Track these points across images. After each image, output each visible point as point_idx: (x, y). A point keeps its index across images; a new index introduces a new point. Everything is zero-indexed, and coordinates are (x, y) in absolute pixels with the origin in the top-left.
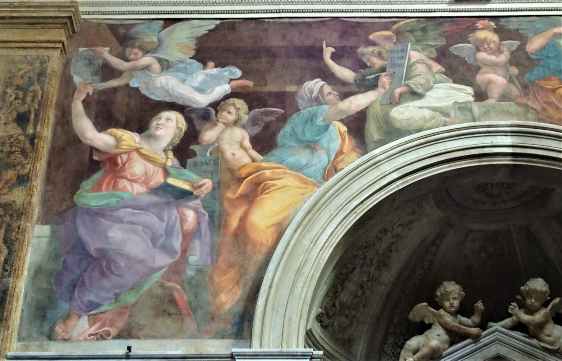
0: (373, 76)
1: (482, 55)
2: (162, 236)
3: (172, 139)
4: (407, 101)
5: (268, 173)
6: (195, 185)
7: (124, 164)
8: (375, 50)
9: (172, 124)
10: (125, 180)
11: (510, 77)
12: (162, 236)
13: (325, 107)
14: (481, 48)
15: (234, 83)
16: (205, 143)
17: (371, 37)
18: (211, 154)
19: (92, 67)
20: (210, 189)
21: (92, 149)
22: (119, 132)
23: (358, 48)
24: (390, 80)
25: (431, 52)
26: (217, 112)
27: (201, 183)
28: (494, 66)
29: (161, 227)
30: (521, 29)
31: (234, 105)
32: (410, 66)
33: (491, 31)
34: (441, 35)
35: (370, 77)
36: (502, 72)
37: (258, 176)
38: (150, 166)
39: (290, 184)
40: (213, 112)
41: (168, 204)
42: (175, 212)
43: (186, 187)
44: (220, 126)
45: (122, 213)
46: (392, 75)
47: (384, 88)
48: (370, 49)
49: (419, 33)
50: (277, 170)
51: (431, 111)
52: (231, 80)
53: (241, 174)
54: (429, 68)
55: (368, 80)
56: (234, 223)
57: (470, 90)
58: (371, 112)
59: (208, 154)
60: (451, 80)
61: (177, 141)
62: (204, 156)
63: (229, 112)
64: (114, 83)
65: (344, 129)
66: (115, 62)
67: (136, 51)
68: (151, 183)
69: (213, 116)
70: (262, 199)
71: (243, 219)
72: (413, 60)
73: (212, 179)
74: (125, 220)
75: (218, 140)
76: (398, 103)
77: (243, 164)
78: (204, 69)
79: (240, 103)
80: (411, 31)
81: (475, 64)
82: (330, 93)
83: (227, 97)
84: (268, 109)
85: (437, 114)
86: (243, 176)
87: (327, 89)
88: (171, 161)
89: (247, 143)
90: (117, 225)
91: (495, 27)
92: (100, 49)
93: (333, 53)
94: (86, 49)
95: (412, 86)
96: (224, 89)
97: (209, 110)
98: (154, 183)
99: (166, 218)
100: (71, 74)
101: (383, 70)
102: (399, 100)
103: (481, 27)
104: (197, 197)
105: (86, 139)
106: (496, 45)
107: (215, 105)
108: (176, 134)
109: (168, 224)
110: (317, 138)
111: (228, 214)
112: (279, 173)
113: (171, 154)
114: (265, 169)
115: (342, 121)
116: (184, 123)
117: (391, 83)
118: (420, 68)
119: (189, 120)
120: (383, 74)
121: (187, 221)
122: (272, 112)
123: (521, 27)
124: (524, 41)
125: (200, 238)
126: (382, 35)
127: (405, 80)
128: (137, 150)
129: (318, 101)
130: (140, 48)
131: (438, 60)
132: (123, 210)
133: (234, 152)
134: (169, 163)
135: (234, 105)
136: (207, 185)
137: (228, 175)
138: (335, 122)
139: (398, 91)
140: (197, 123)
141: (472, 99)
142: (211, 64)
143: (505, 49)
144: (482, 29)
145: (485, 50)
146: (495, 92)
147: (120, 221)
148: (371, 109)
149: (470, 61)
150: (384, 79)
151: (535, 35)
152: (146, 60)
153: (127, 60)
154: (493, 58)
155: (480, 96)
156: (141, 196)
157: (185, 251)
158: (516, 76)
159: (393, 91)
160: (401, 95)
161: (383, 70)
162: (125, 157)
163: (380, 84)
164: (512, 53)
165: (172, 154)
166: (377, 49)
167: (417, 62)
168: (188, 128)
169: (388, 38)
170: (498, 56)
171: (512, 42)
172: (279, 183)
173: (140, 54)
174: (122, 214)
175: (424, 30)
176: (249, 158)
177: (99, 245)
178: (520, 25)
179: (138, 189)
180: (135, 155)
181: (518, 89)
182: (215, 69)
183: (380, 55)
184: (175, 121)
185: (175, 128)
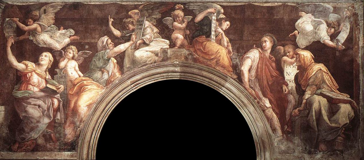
0: (129, 35)
1: (176, 24)
2: (45, 110)
3: (48, 66)
4: (141, 47)
5: (85, 82)
6: (57, 88)
7: (30, 78)
8: (131, 20)
9: (47, 59)
10: (31, 85)
11: (186, 36)
12: (45, 110)
13: (108, 50)
14: (176, 20)
15: (72, 37)
16: (61, 68)
17: (129, 13)
18: (63, 73)
19: (12, 28)
20: (63, 90)
21: (17, 71)
22: (27, 62)
23: (124, 19)
24: (135, 37)
25: (154, 22)
26: (65, 52)
27: (59, 87)
28: (180, 29)
29: (45, 107)
30: (194, 10)
31: (72, 49)
32: (145, 29)
33: (181, 10)
34: (159, 12)
35: (127, 35)
36: (182, 32)
37: (81, 84)
38: (40, 79)
39: (94, 88)
40: (63, 52)
41: (47, 96)
42: (50, 100)
43: (54, 88)
44: (66, 60)
45: (30, 100)
46: (136, 35)
47: (133, 41)
48: (129, 20)
49: (150, 11)
50: (89, 81)
51: (151, 53)
52: (71, 36)
53: (75, 83)
54: (153, 30)
55: (127, 36)
56: (72, 105)
57: (168, 42)
58: (127, 53)
59: (62, 73)
60: (161, 37)
61: (50, 67)
62: (61, 74)
63: (70, 53)
64: (22, 38)
65: (115, 61)
66: (22, 25)
67: (30, 20)
68: (40, 87)
69: (63, 55)
70: (83, 94)
71: (76, 103)
72: (146, 26)
73: (64, 85)
74: (32, 103)
75: (66, 66)
76: (138, 48)
77: (76, 78)
78: (59, 30)
79: (74, 48)
80: (147, 10)
81: (172, 29)
82: (110, 43)
83: (68, 45)
84: (85, 51)
85: (153, 54)
86: (76, 84)
87: (110, 41)
88: (48, 77)
89: (77, 68)
90: (29, 106)
91: (183, 8)
92: (15, 19)
93: (113, 21)
94: (9, 19)
95: (145, 40)
96: (67, 40)
97: (62, 52)
98: (41, 87)
99: (47, 103)
100: (4, 33)
101: (133, 30)
102: (139, 47)
103: (177, 8)
104: (58, 93)
105: (14, 66)
106: (182, 18)
107: (64, 49)
108: (49, 63)
109: (48, 105)
110: (104, 66)
111: (70, 101)
112: (88, 82)
113: (48, 73)
114: (85, 80)
115: (115, 57)
116: (52, 58)
117: (136, 38)
118: (149, 30)
119: (54, 56)
120: (133, 33)
121: (55, 104)
122: (87, 53)
123: (194, 8)
124: (195, 16)
125: (60, 111)
126: (134, 12)
127: (142, 37)
128: (34, 71)
129: (105, 48)
130: (31, 18)
131: (156, 26)
132: (31, 99)
133: (71, 72)
134: (47, 77)
135: (72, 49)
136: (62, 87)
137: (70, 83)
138: (112, 58)
139: (139, 42)
140: (57, 58)
141: (168, 47)
142: (62, 28)
143: (186, 20)
144: (178, 9)
145: (177, 21)
146: (179, 43)
147: (30, 103)
148: (127, 51)
149: (170, 27)
150: (134, 36)
151: (199, 13)
152: (35, 26)
153: (27, 25)
154: (180, 25)
155: (172, 45)
156: (37, 93)
157: (55, 116)
158: (188, 35)
159: (136, 43)
160: (140, 44)
161: (133, 30)
162: (30, 74)
163: (131, 39)
164: (188, 22)
165: (48, 73)
166: (131, 20)
167: (147, 27)
168: (54, 60)
169: (135, 14)
170: (182, 24)
171: (189, 16)
172: (89, 87)
173: (32, 22)
174: (31, 101)
175: (152, 9)
176: (78, 75)
177: (24, 114)
178: (194, 7)
179: (36, 89)
180: (33, 73)
181: (188, 42)
182: (64, 31)
183: (132, 23)
184: (48, 57)
185: (49, 60)
